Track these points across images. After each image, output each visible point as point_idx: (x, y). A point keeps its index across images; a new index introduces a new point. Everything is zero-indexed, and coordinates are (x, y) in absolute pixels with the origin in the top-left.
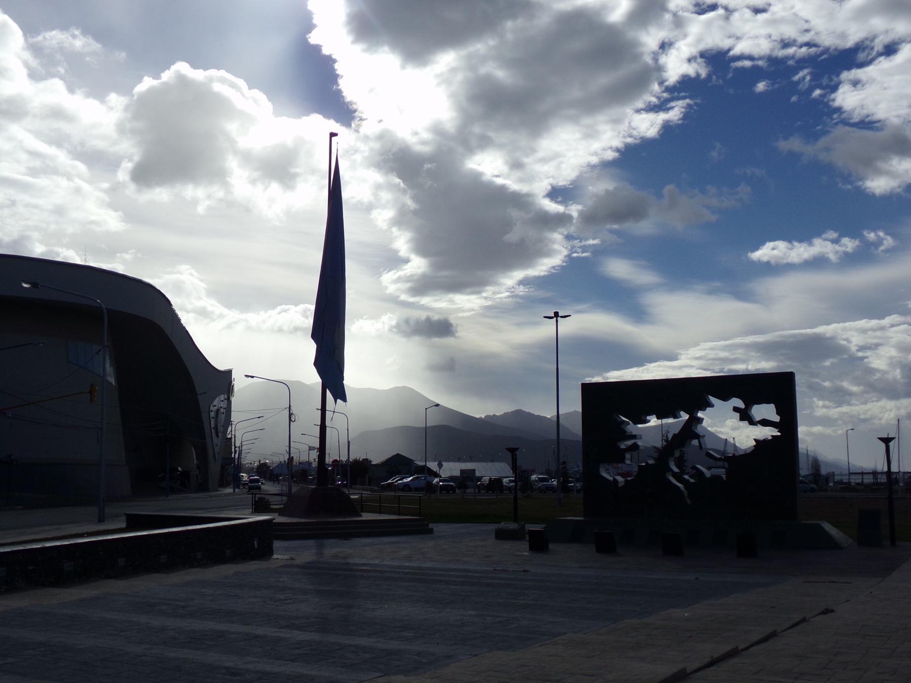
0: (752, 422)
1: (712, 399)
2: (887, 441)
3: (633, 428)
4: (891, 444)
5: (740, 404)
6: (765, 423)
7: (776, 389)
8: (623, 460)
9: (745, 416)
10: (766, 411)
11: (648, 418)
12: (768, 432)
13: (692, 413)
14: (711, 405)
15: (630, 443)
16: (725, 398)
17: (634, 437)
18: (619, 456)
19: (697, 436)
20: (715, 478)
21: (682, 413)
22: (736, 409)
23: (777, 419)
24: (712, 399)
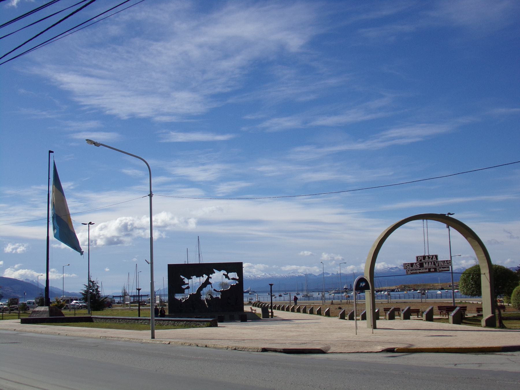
0: (229, 279)
2: (271, 285)
3: (186, 280)
4: (273, 286)
7: (237, 267)
9: (227, 276)
10: (233, 275)
12: (234, 283)
13: (208, 276)
14: (214, 273)
15: (186, 286)
16: (220, 270)
17: (188, 284)
18: (182, 291)
19: (210, 284)
21: (204, 275)
22: (224, 274)
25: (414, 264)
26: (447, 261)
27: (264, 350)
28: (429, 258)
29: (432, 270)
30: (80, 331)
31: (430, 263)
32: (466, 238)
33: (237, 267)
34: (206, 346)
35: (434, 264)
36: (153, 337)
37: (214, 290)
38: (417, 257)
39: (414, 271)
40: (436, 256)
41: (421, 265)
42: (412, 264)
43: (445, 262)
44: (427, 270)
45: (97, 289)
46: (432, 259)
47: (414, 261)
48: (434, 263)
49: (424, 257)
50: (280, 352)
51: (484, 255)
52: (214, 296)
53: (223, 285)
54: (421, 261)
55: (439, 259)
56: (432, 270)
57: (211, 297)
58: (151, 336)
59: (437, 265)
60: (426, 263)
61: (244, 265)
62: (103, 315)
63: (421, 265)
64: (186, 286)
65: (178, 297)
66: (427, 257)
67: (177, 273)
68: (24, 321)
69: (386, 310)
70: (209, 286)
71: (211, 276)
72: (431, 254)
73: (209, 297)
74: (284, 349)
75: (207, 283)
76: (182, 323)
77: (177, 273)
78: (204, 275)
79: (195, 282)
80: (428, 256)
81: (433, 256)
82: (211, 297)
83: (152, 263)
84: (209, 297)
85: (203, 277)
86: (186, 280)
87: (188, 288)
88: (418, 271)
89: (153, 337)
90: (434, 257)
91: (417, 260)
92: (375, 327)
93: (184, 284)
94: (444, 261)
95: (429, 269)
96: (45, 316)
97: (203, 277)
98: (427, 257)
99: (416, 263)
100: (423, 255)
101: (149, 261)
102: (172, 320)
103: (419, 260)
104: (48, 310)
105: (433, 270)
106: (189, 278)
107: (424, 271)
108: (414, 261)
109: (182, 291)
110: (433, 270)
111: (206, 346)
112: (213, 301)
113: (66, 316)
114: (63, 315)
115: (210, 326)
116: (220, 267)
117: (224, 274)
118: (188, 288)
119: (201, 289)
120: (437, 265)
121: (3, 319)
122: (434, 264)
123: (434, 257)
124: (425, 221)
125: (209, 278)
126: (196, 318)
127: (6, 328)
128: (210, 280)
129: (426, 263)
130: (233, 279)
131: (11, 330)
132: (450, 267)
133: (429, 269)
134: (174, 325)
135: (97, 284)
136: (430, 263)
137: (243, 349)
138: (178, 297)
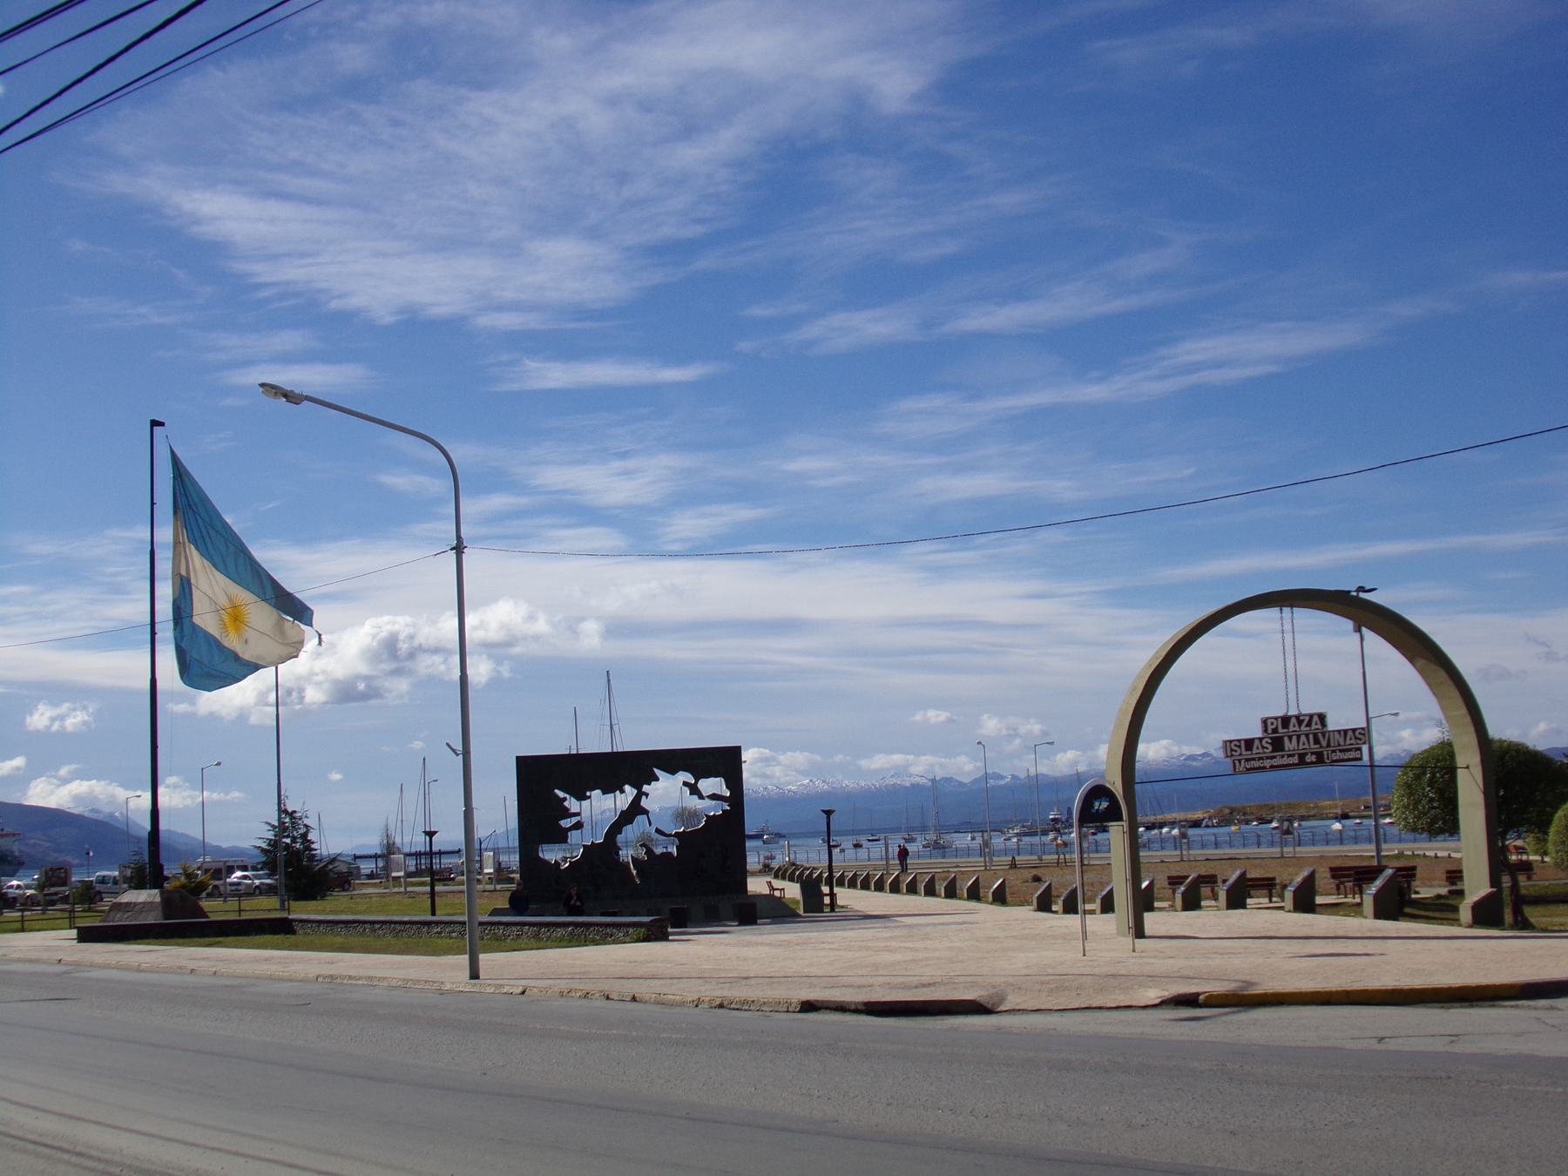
0: (701, 797)
2: (828, 813)
3: (572, 804)
7: (725, 762)
9: (694, 790)
10: (713, 785)
12: (716, 809)
13: (639, 788)
14: (657, 779)
15: (574, 820)
16: (672, 771)
17: (578, 814)
18: (561, 837)
19: (646, 812)
21: (627, 788)
22: (685, 784)
25: (1257, 743)
26: (1354, 730)
27: (809, 1007)
28: (1300, 722)
29: (1309, 758)
30: (257, 960)
31: (1303, 738)
32: (1411, 660)
33: (725, 762)
34: (634, 999)
35: (1317, 741)
36: (475, 975)
37: (658, 831)
38: (1265, 722)
39: (1257, 764)
40: (1322, 717)
41: (1277, 744)
42: (1249, 743)
43: (1350, 734)
44: (1295, 760)
45: (304, 836)
46: (1309, 724)
47: (1256, 732)
48: (1315, 736)
49: (1285, 720)
50: (856, 1011)
51: (1464, 711)
52: (658, 851)
53: (684, 815)
54: (1275, 731)
55: (1332, 725)
56: (1309, 758)
57: (649, 852)
58: (467, 973)
59: (1324, 743)
60: (1290, 738)
61: (746, 756)
62: (324, 912)
63: (1277, 744)
64: (574, 820)
65: (551, 854)
66: (1293, 720)
67: (546, 782)
68: (87, 935)
69: (1175, 881)
70: (641, 819)
71: (646, 788)
72: (1307, 709)
73: (642, 854)
74: (867, 1004)
75: (635, 809)
76: (560, 932)
77: (546, 782)
78: (627, 788)
79: (599, 808)
80: (1297, 717)
81: (1311, 716)
82: (649, 852)
83: (466, 753)
84: (642, 854)
85: (622, 791)
86: (572, 804)
87: (579, 826)
88: (1267, 763)
89: (475, 975)
90: (1316, 718)
91: (1265, 730)
92: (1139, 933)
93: (567, 814)
94: (1346, 731)
95: (1302, 756)
96: (152, 918)
97: (622, 791)
98: (1293, 720)
99: (1261, 739)
100: (1281, 714)
101: (459, 747)
102: (531, 924)
103: (1270, 728)
104: (158, 899)
105: (1314, 758)
106: (581, 797)
107: (1285, 761)
108: (1256, 732)
109: (561, 837)
110: (1314, 758)
111: (634, 999)
112: (653, 864)
113: (213, 917)
114: (204, 915)
115: (646, 939)
116: (673, 760)
117: (685, 784)
118: (579, 826)
119: (616, 828)
120: (1324, 743)
121: (23, 930)
122: (1317, 741)
123: (1316, 718)
124: (1286, 610)
126: (603, 914)
127: (34, 955)
128: (644, 803)
129: (1290, 738)
130: (714, 797)
131: (45, 962)
132: (1365, 748)
133: (1302, 756)
134: (537, 936)
135: (306, 821)
136: (1303, 738)
137: (744, 1005)
138: (551, 854)
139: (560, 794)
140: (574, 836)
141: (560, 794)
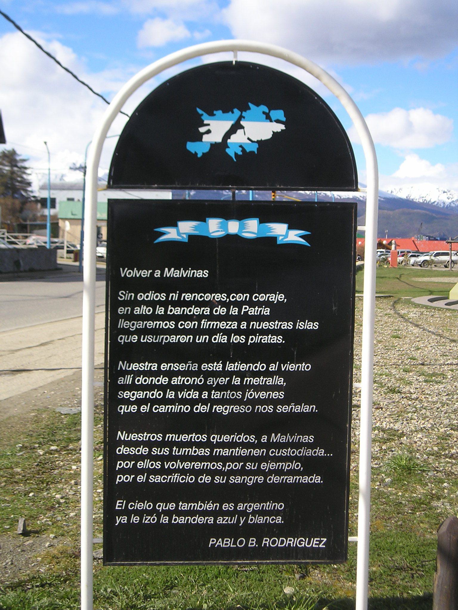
0: (271, 121)
1: (250, 104)
5: (267, 110)
6: (278, 121)
8: (200, 139)
11: (215, 112)
16: (258, 105)
17: (209, 125)
18: (199, 137)
19: (243, 127)
20: (252, 153)
22: (264, 113)
23: (284, 119)
24: (250, 104)
37: (248, 139)
71: (244, 114)
78: (236, 110)
82: (243, 150)
85: (233, 112)
87: (209, 132)
97: (233, 112)
112: (245, 156)
117: (264, 113)
119: (228, 135)
125: (241, 118)
128: (242, 123)
139: (200, 111)
140: (206, 138)
141: (200, 111)
